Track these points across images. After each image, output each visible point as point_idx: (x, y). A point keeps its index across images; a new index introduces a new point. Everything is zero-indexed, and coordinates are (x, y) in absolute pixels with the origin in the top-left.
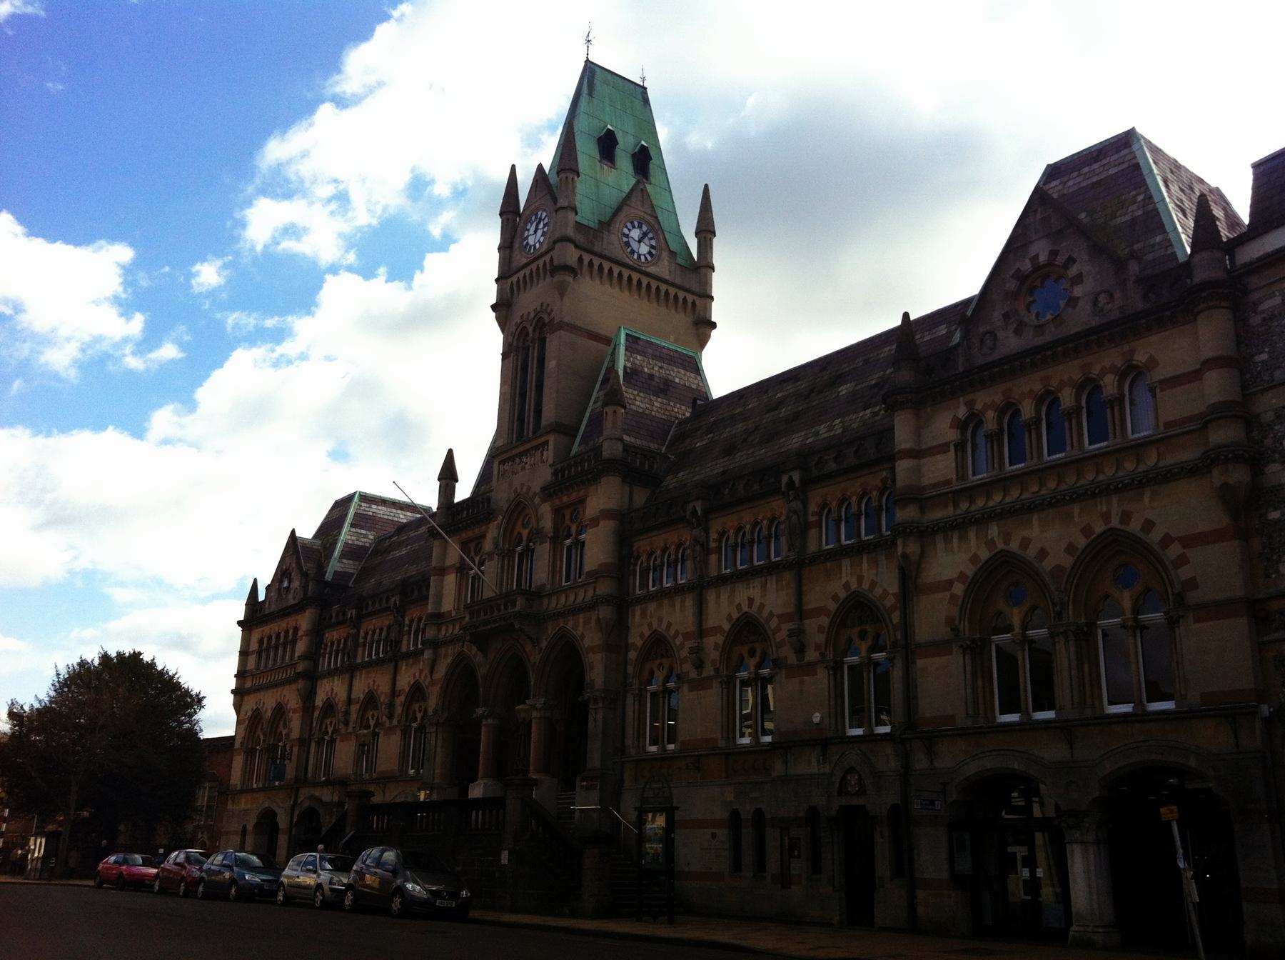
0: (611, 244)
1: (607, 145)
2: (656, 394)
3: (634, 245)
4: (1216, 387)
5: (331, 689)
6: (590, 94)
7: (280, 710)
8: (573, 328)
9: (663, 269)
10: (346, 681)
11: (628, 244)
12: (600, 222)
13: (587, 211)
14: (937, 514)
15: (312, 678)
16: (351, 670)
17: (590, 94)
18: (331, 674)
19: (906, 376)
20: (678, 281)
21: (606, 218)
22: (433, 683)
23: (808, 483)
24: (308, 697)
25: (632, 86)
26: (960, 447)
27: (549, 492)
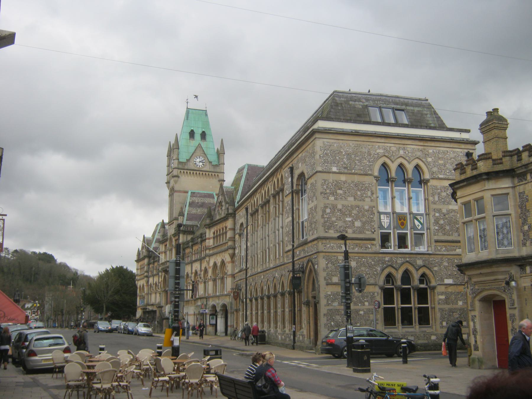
0: (191, 166)
1: (192, 134)
2: (199, 207)
3: (198, 163)
4: (229, 234)
5: (151, 280)
6: (187, 119)
7: (143, 285)
8: (179, 191)
9: (207, 168)
10: (199, 264)
11: (196, 164)
12: (187, 160)
13: (183, 158)
14: (211, 252)
15: (147, 277)
16: (153, 276)
17: (187, 119)
18: (150, 277)
19: (208, 221)
20: (213, 170)
21: (188, 158)
22: (210, 267)
23: (202, 241)
24: (148, 282)
25: (202, 112)
26: (214, 238)
27: (174, 235)
